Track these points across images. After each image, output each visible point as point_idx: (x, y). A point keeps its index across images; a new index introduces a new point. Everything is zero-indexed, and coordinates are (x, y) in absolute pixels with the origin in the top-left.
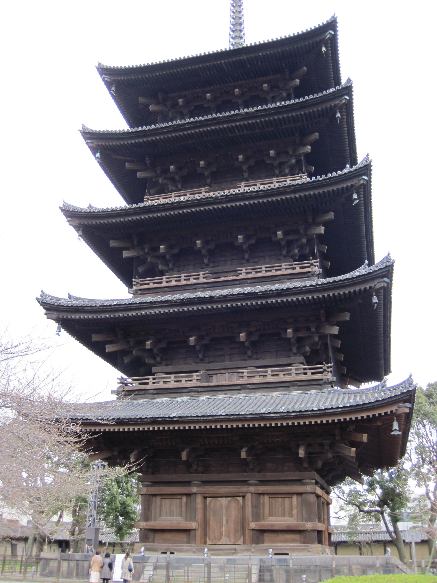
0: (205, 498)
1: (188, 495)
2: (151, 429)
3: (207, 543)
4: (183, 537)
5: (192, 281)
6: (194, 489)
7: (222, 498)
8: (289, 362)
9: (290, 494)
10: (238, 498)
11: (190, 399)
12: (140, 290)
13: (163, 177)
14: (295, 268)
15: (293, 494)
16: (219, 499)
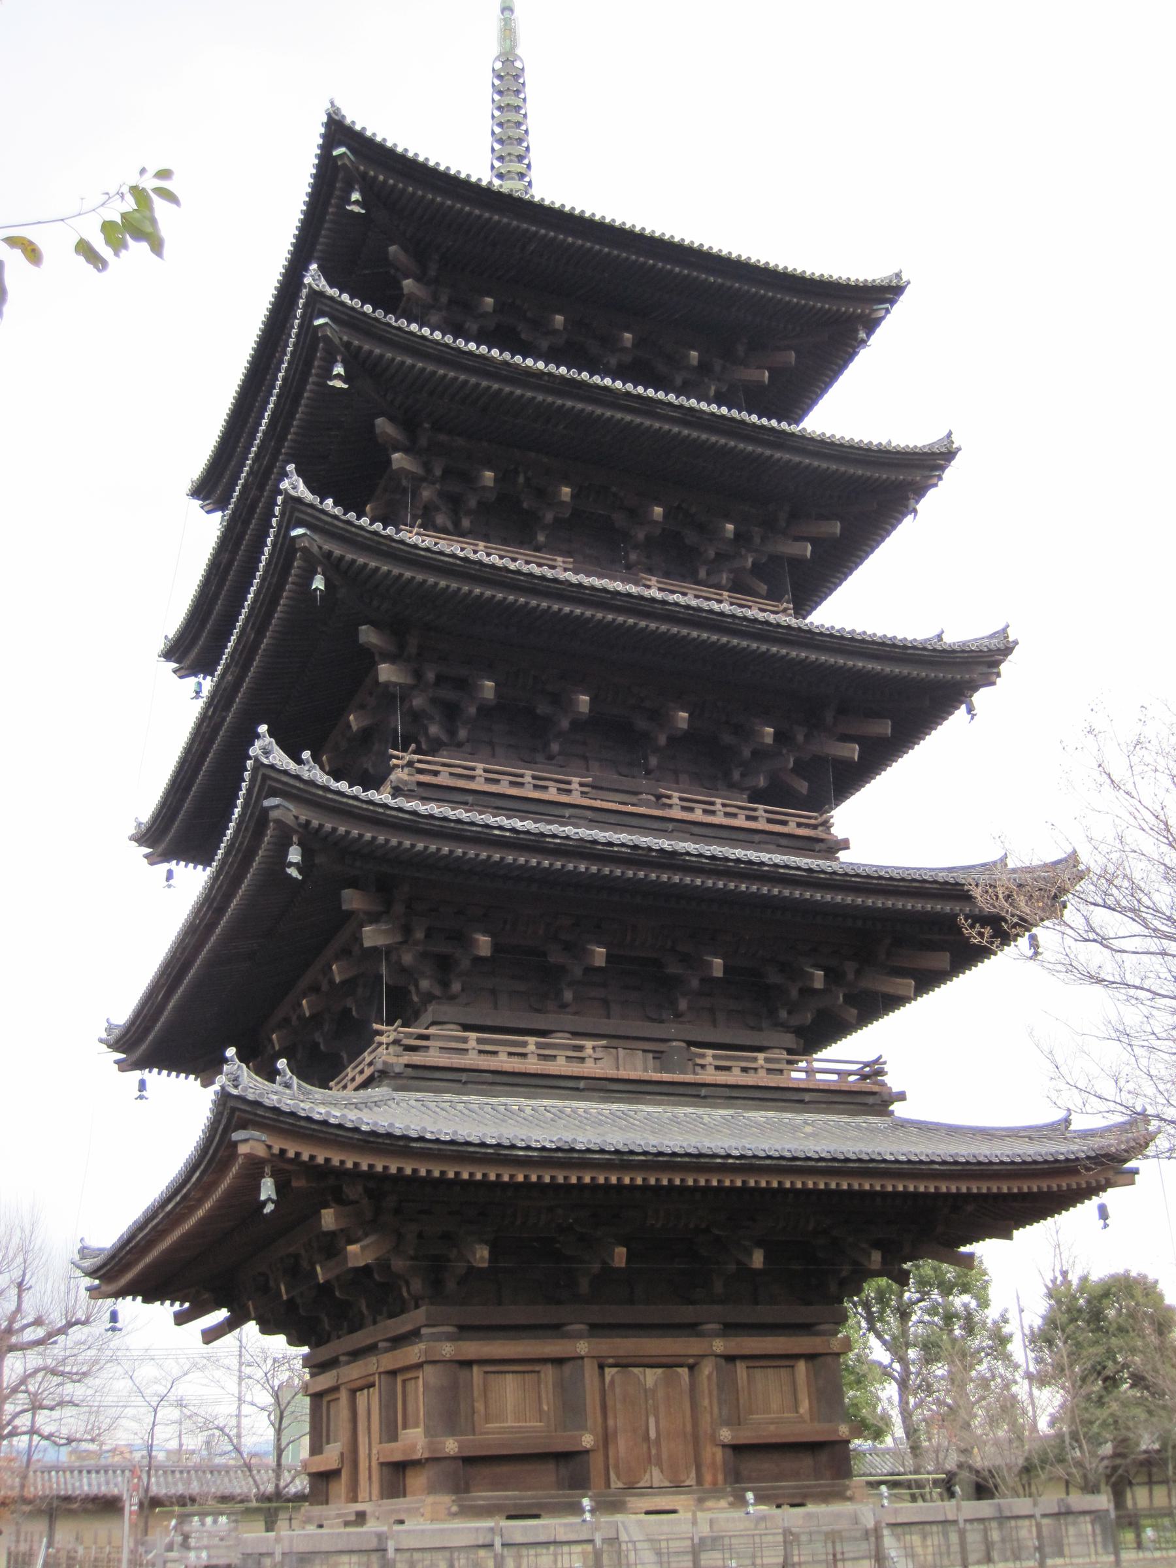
0: (601, 1367)
1: (559, 1362)
2: (520, 1178)
3: (613, 1486)
4: (548, 1473)
5: (552, 794)
6: (582, 1347)
7: (641, 1369)
8: (765, 1044)
9: (789, 1358)
10: (680, 1370)
11: (581, 1106)
12: (420, 784)
13: (438, 486)
14: (785, 823)
15: (797, 1357)
16: (636, 1370)
